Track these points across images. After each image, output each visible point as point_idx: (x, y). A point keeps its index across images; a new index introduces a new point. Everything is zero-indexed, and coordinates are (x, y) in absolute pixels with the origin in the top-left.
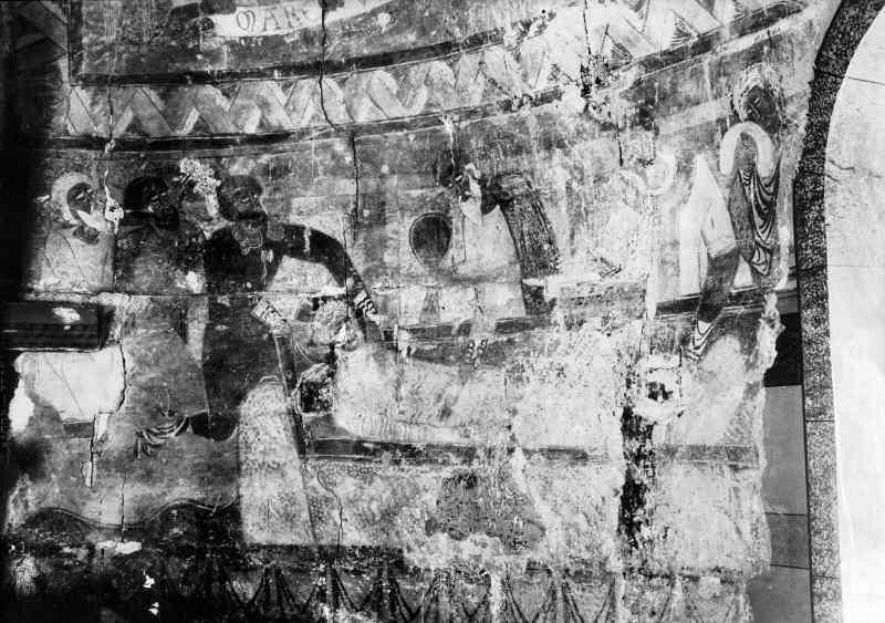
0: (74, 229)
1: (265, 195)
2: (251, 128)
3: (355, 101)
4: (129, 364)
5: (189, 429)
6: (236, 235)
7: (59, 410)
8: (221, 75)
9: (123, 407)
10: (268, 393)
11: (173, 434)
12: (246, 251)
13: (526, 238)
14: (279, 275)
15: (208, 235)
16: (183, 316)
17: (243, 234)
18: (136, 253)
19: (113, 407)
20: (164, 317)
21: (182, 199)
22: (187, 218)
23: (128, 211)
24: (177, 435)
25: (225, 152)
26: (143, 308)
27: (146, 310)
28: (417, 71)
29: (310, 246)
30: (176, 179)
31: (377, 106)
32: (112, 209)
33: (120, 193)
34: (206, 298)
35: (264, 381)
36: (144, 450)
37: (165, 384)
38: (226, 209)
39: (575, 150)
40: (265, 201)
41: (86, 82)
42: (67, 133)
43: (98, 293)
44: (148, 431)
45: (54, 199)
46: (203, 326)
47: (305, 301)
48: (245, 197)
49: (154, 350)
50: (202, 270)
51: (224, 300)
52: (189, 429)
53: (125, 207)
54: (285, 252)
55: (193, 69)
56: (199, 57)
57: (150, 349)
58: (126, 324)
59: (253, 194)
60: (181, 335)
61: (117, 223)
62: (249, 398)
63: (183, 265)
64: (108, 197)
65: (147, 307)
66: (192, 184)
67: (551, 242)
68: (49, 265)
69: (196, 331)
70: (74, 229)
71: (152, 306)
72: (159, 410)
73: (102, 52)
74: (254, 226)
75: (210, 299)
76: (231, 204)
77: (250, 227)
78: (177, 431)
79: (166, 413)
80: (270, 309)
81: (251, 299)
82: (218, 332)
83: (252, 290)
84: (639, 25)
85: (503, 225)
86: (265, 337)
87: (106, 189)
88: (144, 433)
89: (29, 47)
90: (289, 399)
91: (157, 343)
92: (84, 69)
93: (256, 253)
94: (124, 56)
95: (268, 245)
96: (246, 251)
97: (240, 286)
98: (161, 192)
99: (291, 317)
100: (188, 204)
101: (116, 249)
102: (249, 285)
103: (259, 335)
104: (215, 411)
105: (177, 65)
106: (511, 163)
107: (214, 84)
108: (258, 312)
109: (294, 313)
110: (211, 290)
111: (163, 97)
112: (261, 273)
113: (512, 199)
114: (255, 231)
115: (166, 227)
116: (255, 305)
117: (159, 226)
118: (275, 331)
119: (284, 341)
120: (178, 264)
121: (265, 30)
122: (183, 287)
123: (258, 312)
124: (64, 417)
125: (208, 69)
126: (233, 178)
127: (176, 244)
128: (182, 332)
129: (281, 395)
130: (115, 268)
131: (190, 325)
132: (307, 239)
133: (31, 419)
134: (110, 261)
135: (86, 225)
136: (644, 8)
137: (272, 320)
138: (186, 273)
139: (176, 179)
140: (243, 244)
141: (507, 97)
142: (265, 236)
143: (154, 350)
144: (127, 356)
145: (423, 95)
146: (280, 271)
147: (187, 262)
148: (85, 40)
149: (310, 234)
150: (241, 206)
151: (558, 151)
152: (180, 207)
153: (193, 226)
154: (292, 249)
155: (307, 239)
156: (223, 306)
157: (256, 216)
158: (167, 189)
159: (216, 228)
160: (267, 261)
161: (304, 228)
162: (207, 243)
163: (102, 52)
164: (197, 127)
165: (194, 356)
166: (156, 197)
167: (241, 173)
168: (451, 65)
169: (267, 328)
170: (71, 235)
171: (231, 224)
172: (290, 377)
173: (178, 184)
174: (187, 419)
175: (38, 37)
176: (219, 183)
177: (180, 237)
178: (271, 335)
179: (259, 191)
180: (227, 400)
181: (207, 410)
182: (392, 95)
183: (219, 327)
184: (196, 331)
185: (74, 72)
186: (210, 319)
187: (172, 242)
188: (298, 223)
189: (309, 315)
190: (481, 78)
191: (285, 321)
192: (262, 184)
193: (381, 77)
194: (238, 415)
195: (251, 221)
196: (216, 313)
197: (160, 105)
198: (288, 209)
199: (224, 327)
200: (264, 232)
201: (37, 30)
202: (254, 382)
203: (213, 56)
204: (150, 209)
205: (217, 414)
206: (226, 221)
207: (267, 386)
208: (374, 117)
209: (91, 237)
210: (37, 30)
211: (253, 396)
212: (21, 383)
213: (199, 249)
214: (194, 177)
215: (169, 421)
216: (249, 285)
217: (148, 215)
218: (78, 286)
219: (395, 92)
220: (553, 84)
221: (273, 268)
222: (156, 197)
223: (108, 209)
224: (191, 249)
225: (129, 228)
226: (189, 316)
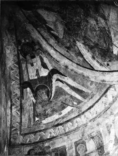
2: (48, 137)
3: (65, 129)
8: (43, 130)
13: (97, 143)
25: (44, 142)
28: (75, 121)
31: (69, 128)
39: (102, 124)
41: (22, 135)
42: (19, 143)
55: (39, 130)
56: (40, 128)
67: (101, 142)
73: (25, 130)
84: (107, 99)
85: (93, 143)
89: (14, 130)
92: (22, 133)
94: (28, 130)
105: (37, 130)
106: (93, 130)
107: (42, 131)
111: (34, 135)
113: (94, 137)
121: (50, 121)
125: (41, 129)
136: (107, 96)
141: (90, 120)
145: (76, 124)
148: (22, 128)
151: (100, 125)
163: (25, 130)
164: (40, 139)
168: (80, 118)
175: (15, 128)
182: (71, 126)
185: (20, 133)
190: (85, 118)
193: (70, 123)
197: (34, 136)
201: (15, 127)
203: (42, 127)
208: (69, 130)
210: (15, 127)
219: (72, 125)
220: (96, 114)
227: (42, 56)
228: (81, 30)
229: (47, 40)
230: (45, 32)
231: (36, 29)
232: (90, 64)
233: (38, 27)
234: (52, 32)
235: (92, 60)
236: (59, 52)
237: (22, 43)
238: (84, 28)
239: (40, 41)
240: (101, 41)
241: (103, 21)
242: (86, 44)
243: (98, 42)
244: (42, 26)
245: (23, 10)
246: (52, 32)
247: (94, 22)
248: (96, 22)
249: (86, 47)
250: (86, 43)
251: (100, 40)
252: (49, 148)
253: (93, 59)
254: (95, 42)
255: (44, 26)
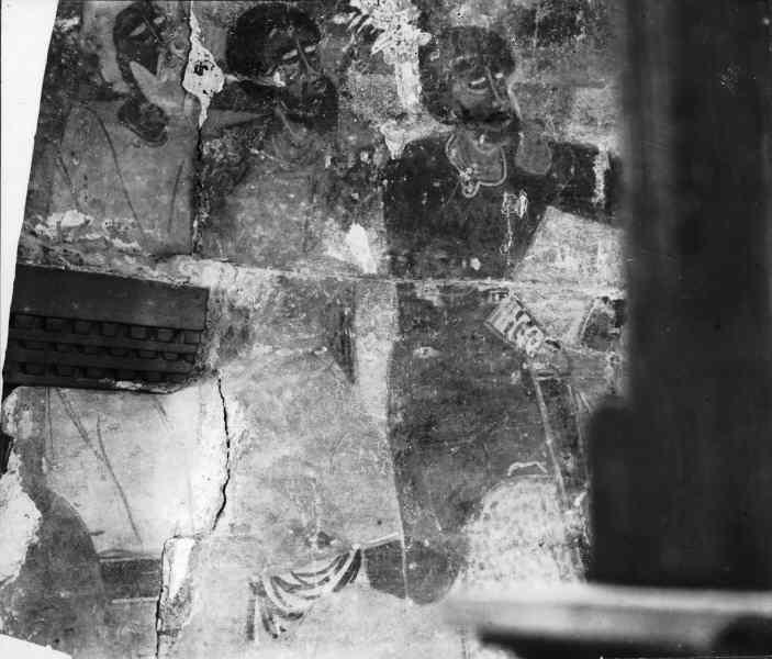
0: (121, 103)
1: (519, 75)
4: (236, 428)
5: (362, 577)
6: (453, 154)
7: (92, 528)
9: (224, 522)
10: (525, 498)
11: (328, 588)
12: (471, 191)
14: (539, 246)
15: (395, 149)
16: (346, 322)
17: (466, 150)
18: (241, 172)
19: (203, 519)
20: (307, 321)
21: (346, 64)
22: (355, 107)
23: (231, 78)
24: (335, 590)
26: (265, 298)
27: (271, 303)
29: (605, 191)
30: (339, 20)
32: (200, 69)
33: (220, 36)
34: (393, 282)
35: (516, 472)
36: (267, 623)
37: (311, 473)
38: (436, 100)
40: (519, 88)
43: (164, 255)
44: (277, 580)
45: (87, 28)
46: (387, 347)
47: (598, 304)
48: (477, 76)
49: (288, 395)
50: (379, 222)
51: (429, 290)
52: (362, 577)
53: (229, 65)
54: (550, 201)
57: (280, 392)
58: (230, 331)
59: (497, 71)
60: (342, 364)
61: (205, 101)
62: (487, 510)
63: (341, 210)
64: (194, 38)
65: (273, 296)
66: (370, 35)
68: (67, 181)
69: (374, 352)
70: (121, 103)
71: (281, 294)
72: (298, 531)
74: (492, 138)
75: (399, 287)
76: (445, 88)
77: (482, 141)
78: (336, 579)
79: (314, 539)
80: (525, 318)
81: (486, 294)
82: (419, 362)
83: (481, 275)
86: (515, 377)
87: (194, 22)
88: (268, 587)
90: (569, 513)
91: (294, 379)
93: (491, 196)
95: (517, 182)
96: (471, 191)
97: (459, 263)
98: (305, 44)
99: (570, 338)
100: (359, 77)
101: (198, 158)
102: (476, 264)
103: (503, 372)
104: (415, 537)
108: (501, 321)
109: (574, 329)
110: (401, 265)
112: (499, 238)
114: (493, 150)
115: (309, 124)
116: (493, 308)
117: (293, 118)
118: (537, 366)
119: (554, 389)
120: (330, 207)
122: (340, 257)
123: (501, 321)
124: (102, 545)
126: (456, 32)
127: (328, 163)
128: (344, 353)
129: (552, 505)
130: (195, 203)
131: (360, 343)
132: (600, 177)
133: (32, 549)
134: (186, 186)
135: (143, 98)
137: (528, 343)
138: (346, 229)
139: (339, 20)
140: (464, 175)
142: (511, 162)
143: (288, 395)
144: (233, 407)
146: (538, 240)
147: (350, 203)
149: (606, 165)
150: (467, 92)
152: (343, 80)
153: (366, 125)
154: (565, 194)
155: (600, 177)
156: (429, 306)
157: (496, 117)
158: (318, 37)
159: (414, 135)
160: (515, 216)
161: (596, 152)
162: (395, 168)
165: (372, 412)
166: (294, 53)
167: (474, 23)
169: (522, 357)
170: (113, 115)
171: (445, 129)
172: (570, 465)
173: (342, 30)
174: (359, 551)
176: (426, 38)
177: (336, 147)
178: (527, 374)
179: (509, 64)
180: (440, 512)
181: (398, 534)
183: (419, 351)
184: (374, 352)
186: (402, 332)
187: (320, 156)
188: (584, 140)
189: (604, 335)
191: (556, 344)
192: (516, 52)
194: (464, 546)
195: (487, 127)
196: (415, 319)
198: (564, 112)
199: (431, 352)
200: (511, 162)
202: (498, 472)
204: (278, 80)
205: (419, 544)
206: (434, 124)
207: (523, 484)
209: (152, 127)
211: (494, 505)
212: (14, 460)
213: (373, 179)
214: (376, 20)
215: (319, 558)
216: (476, 264)
217: (273, 91)
218: (125, 239)
221: (526, 231)
222: (294, 53)
223: (191, 66)
224: (357, 177)
225: (229, 117)
226: (358, 323)
252: (495, 70)
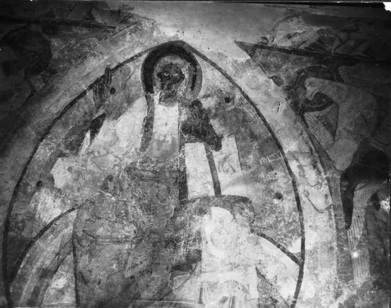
227: (13, 99)
228: (110, 223)
229: (63, 119)
230: (86, 113)
231: (91, 87)
232: (22, 266)
233: (95, 92)
234: (88, 135)
235: (34, 271)
236: (31, 157)
237: (50, 38)
238: (118, 232)
239: (57, 97)
240: (100, 290)
241: (154, 287)
242: (77, 244)
243: (94, 282)
244: (100, 106)
245: (145, 56)
246: (88, 135)
247: (145, 263)
248: (145, 268)
249: (69, 244)
250: (81, 245)
251: (100, 288)
253: (40, 274)
254: (90, 271)
255: (101, 112)
